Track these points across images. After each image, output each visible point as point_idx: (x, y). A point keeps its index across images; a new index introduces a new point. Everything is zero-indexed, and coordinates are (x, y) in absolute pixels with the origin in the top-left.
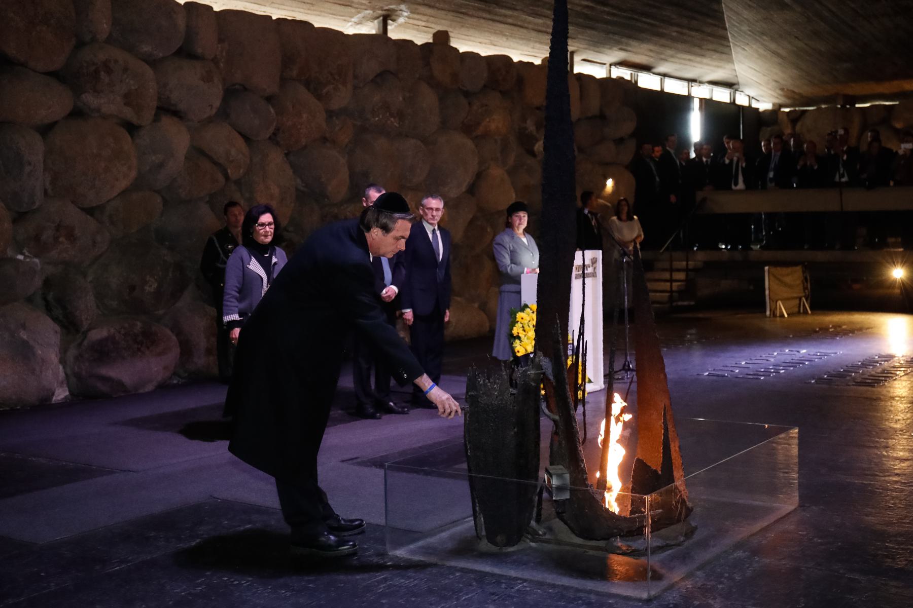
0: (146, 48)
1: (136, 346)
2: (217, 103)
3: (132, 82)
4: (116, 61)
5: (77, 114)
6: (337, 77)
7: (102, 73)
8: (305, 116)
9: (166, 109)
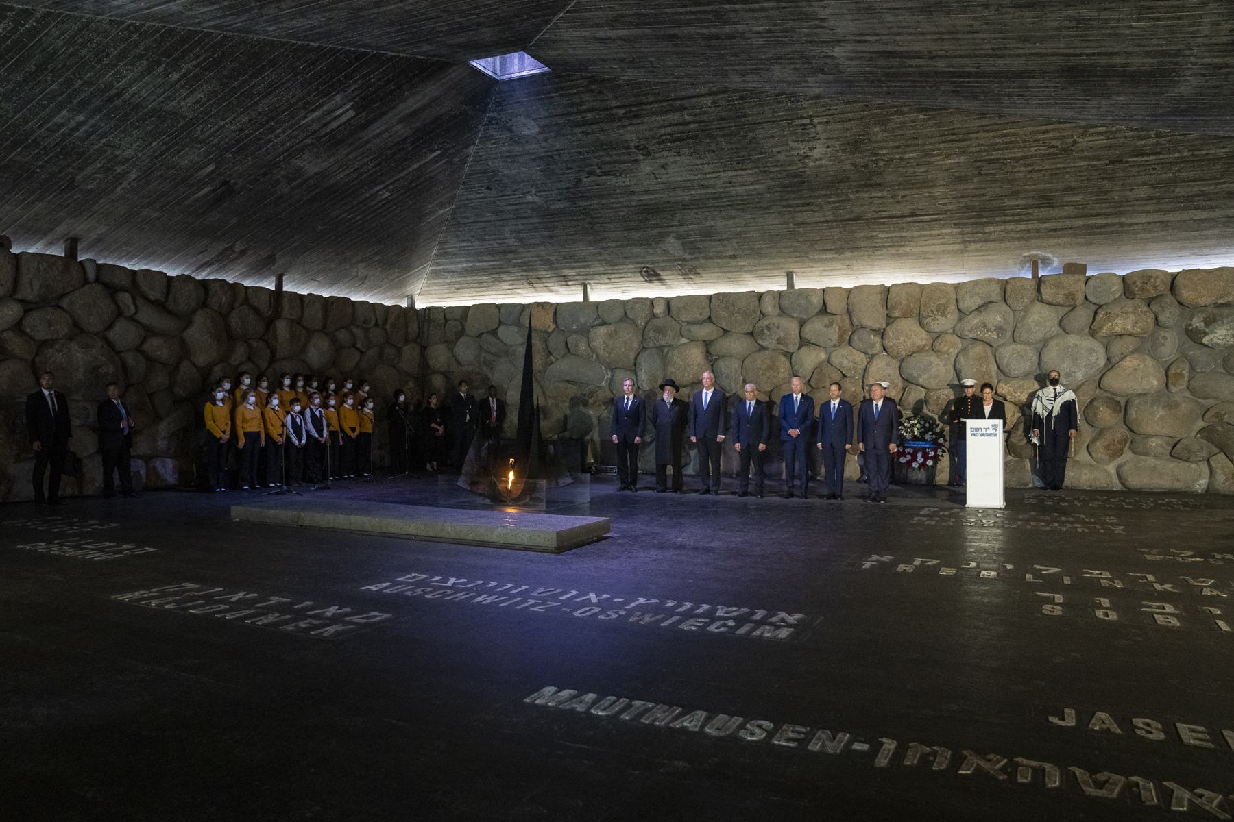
9: (804, 342)
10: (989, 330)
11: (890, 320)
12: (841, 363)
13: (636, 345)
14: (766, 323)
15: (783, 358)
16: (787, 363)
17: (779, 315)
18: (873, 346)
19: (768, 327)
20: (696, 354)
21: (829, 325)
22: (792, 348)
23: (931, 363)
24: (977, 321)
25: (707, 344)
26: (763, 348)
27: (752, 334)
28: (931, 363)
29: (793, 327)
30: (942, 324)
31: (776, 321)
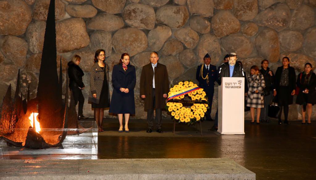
0: (153, 4)
1: (141, 103)
2: (181, 21)
3: (144, 15)
4: (138, 9)
5: (126, 26)
6: (246, 8)
7: (132, 13)
8: (225, 24)
9: (159, 24)
10: (278, 21)
11: (216, 12)
12: (185, 39)
13: (28, 17)
14: (133, 8)
15: (143, 34)
16: (146, 36)
17: (139, 3)
18: (206, 28)
19: (134, 11)
20: (79, 28)
21: (178, 12)
22: (151, 27)
23: (243, 41)
24: (270, 14)
25: (87, 21)
26: (126, 26)
27: (119, 15)
28: (243, 41)
29: (152, 11)
30: (250, 15)
31: (140, 7)
